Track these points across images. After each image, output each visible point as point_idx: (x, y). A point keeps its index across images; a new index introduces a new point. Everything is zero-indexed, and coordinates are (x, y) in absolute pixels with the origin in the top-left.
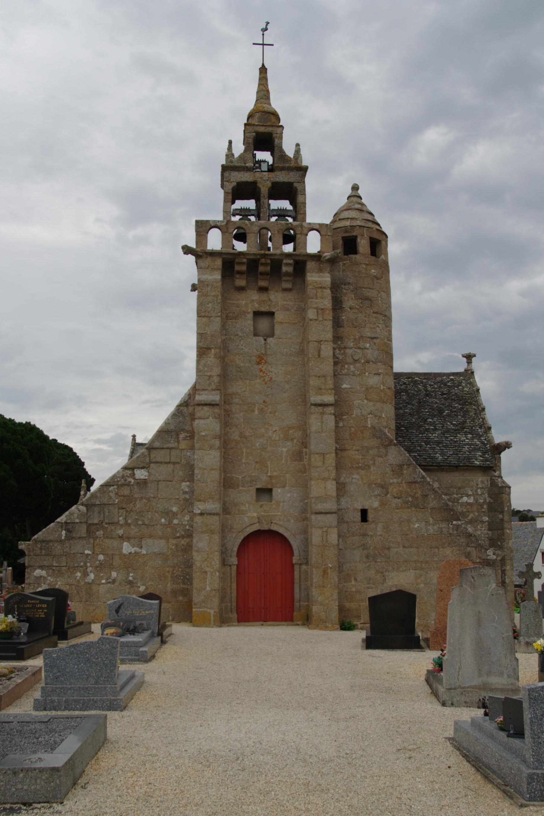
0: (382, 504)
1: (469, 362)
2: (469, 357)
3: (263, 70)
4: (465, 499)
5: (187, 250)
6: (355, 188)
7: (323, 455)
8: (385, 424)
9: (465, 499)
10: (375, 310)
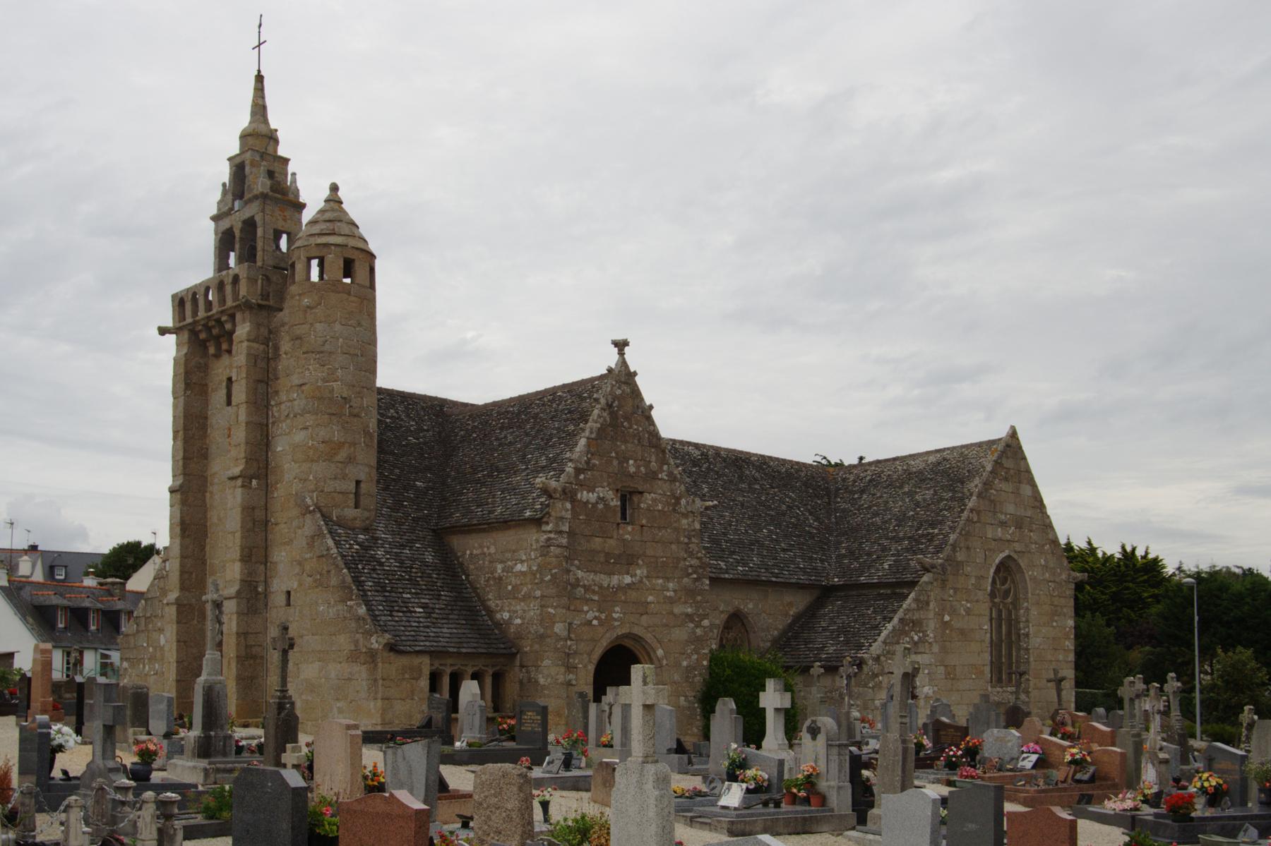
0: (300, 585)
1: (621, 353)
2: (621, 345)
3: (260, 78)
4: (519, 567)
6: (334, 188)
7: (233, 533)
8: (312, 487)
9: (519, 567)
10: (304, 349)
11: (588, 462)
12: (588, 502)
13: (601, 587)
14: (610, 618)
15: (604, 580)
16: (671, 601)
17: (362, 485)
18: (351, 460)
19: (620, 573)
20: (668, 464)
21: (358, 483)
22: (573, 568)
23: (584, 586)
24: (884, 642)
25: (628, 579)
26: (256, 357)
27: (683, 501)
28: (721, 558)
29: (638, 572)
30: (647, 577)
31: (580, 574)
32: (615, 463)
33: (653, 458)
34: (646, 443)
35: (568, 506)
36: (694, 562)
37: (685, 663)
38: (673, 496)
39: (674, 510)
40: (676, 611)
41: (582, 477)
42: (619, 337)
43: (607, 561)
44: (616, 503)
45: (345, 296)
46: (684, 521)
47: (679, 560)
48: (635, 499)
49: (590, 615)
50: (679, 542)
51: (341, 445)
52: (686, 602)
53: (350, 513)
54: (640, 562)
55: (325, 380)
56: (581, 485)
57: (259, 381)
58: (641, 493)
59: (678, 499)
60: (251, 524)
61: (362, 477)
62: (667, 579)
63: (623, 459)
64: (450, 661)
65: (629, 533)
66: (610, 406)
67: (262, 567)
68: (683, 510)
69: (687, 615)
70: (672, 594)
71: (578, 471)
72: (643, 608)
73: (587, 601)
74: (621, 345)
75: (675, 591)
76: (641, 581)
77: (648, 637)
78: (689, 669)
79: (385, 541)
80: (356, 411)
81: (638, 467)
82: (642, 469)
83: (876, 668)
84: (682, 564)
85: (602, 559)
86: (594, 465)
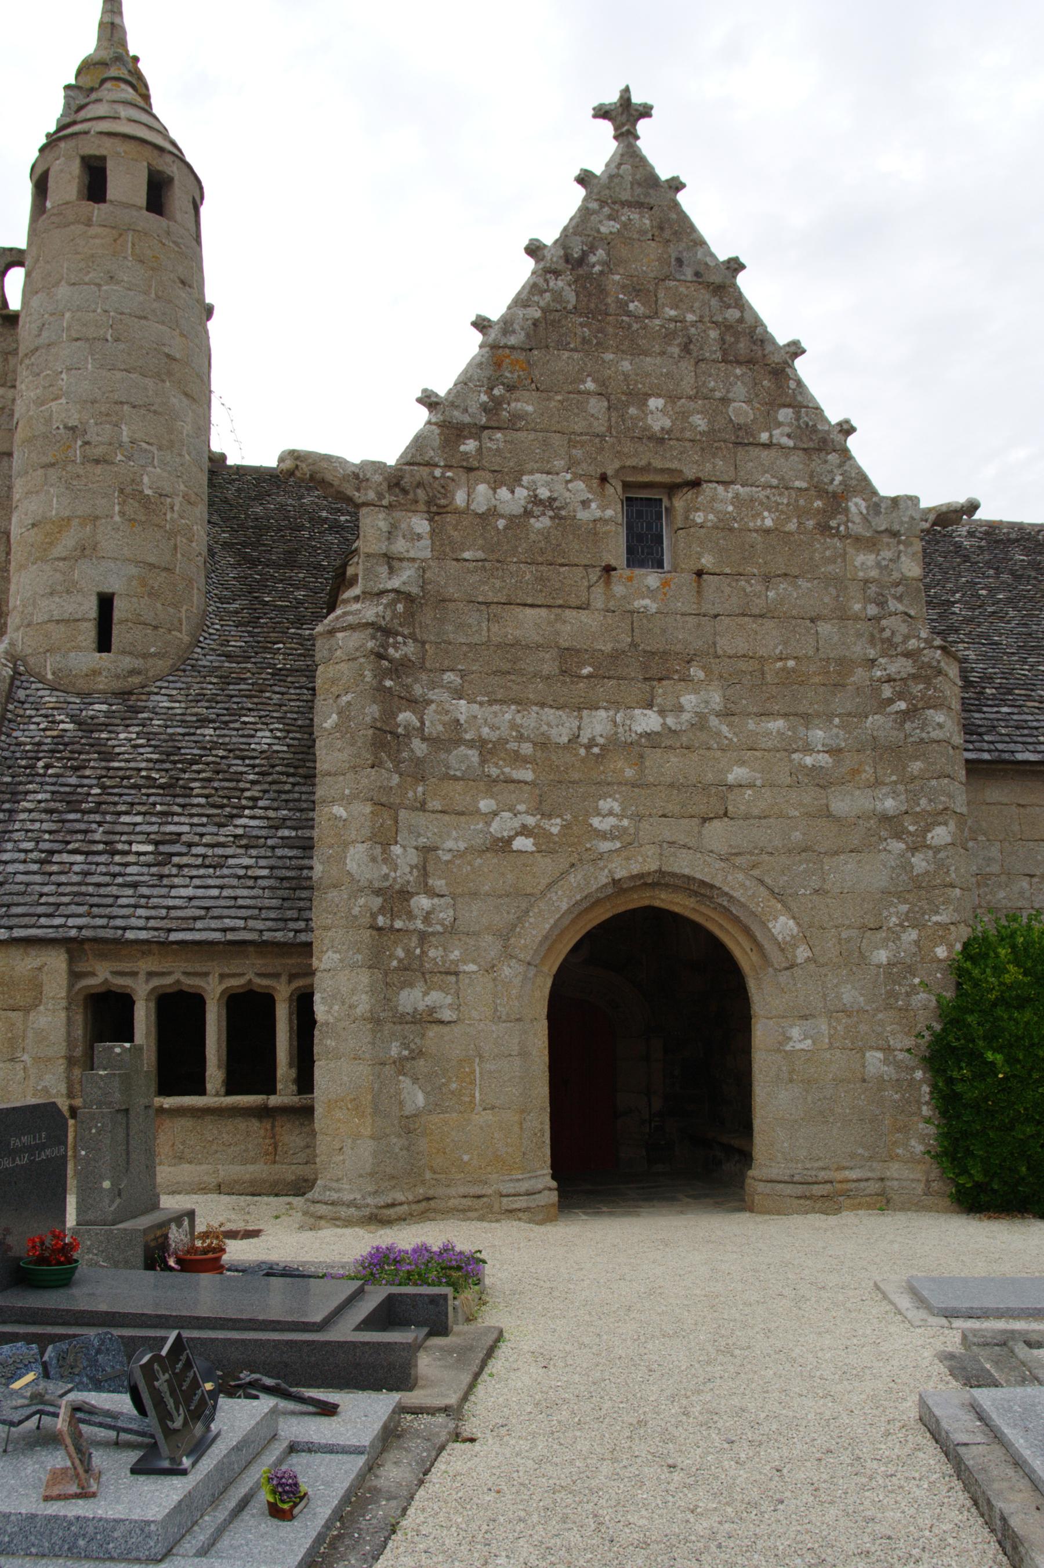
1: (626, 135)
2: (625, 115)
11: (493, 408)
12: (493, 513)
13: (543, 744)
15: (559, 726)
16: (821, 780)
17: (117, 602)
18: (85, 551)
19: (615, 704)
21: (106, 603)
23: (480, 744)
25: (648, 721)
30: (726, 714)
31: (463, 709)
32: (596, 406)
33: (740, 390)
34: (712, 350)
35: (421, 525)
36: (900, 667)
37: (882, 956)
38: (821, 492)
40: (840, 805)
41: (470, 446)
44: (606, 512)
46: (864, 561)
47: (845, 665)
48: (679, 503)
49: (502, 825)
50: (843, 616)
52: (877, 783)
54: (696, 672)
61: (113, 585)
62: (807, 718)
64: (145, 965)
65: (651, 593)
68: (857, 528)
69: (885, 818)
70: (825, 760)
72: (716, 804)
74: (625, 115)
75: (834, 751)
76: (700, 723)
77: (735, 883)
78: (897, 971)
80: (98, 452)
82: (700, 422)
84: (860, 675)
85: (549, 667)
86: (516, 417)
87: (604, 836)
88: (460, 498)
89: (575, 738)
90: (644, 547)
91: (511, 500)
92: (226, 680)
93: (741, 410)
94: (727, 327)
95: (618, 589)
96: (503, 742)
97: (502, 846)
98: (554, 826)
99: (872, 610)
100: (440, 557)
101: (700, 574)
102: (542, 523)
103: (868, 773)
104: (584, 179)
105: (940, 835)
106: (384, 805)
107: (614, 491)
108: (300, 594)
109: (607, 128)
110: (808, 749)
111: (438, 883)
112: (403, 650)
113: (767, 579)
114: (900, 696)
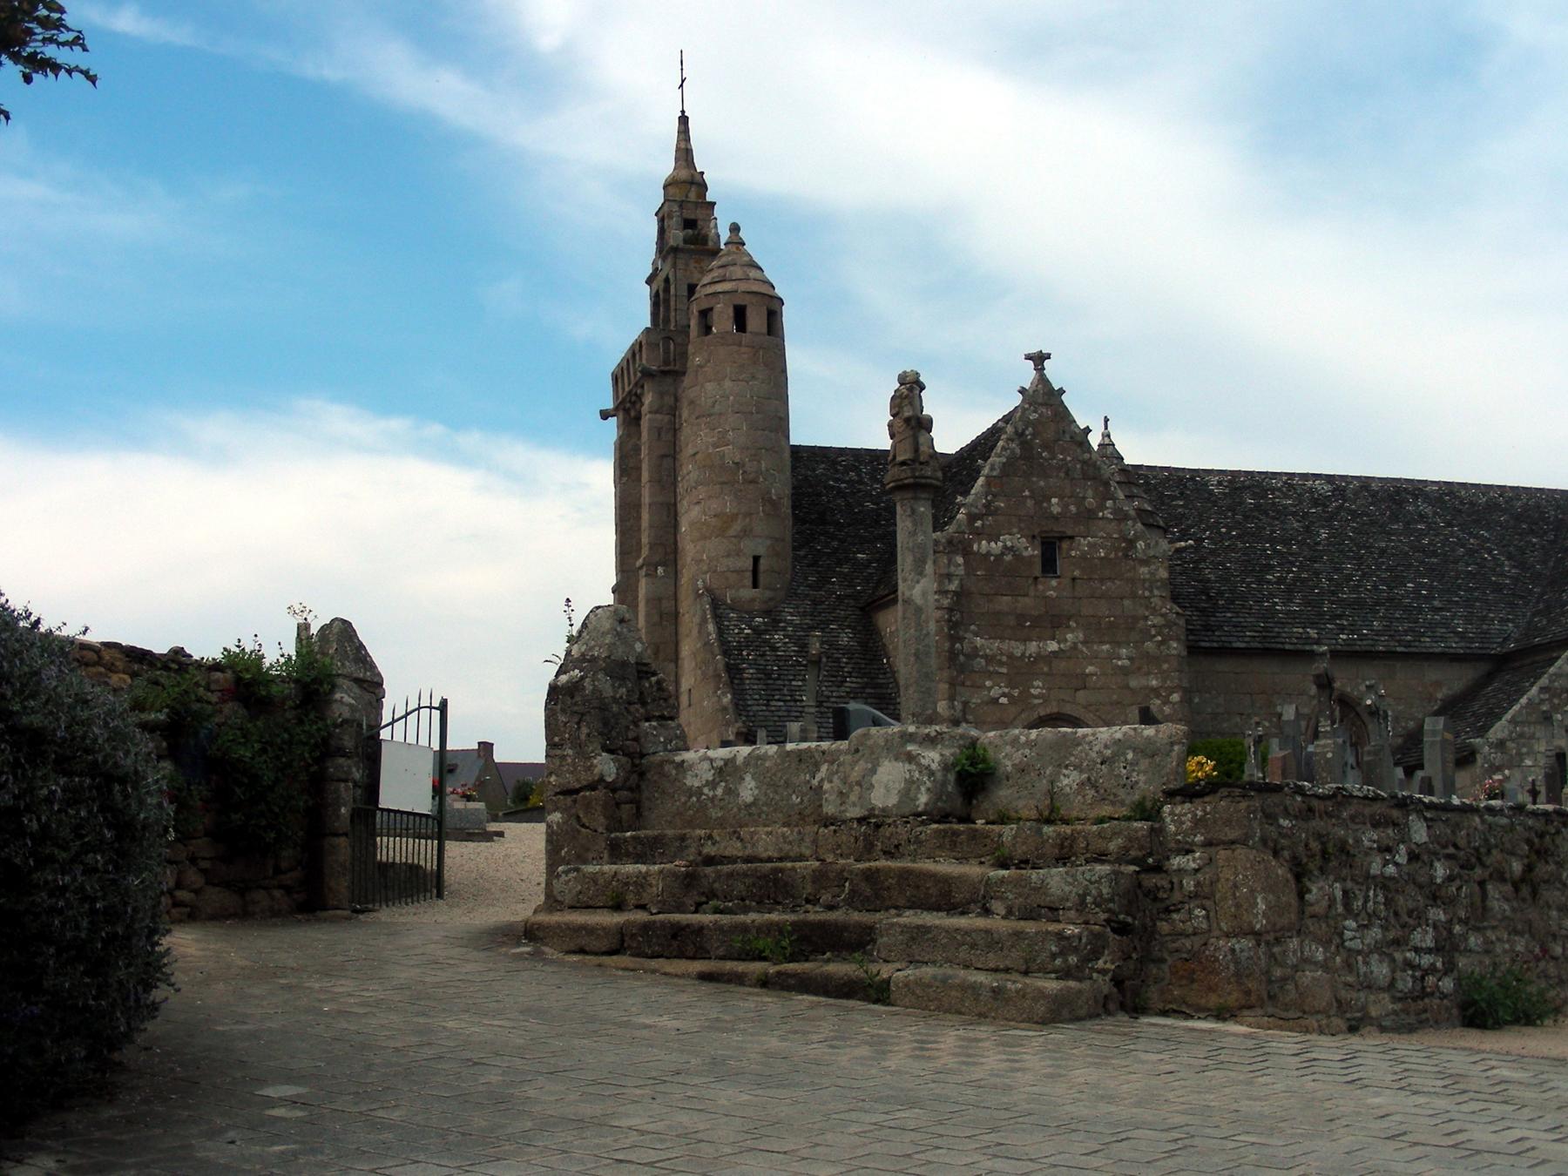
1: (1040, 368)
3: (684, 120)
5: (605, 415)
11: (987, 506)
12: (989, 554)
13: (1011, 656)
14: (1026, 696)
15: (1017, 649)
16: (1125, 671)
17: (762, 561)
18: (745, 533)
19: (1040, 639)
20: (1114, 499)
21: (756, 559)
22: (968, 635)
23: (985, 657)
24: (1513, 721)
25: (1053, 646)
26: (659, 430)
27: (1140, 545)
28: (1313, 625)
29: (1069, 636)
30: (1085, 643)
32: (1030, 503)
33: (1090, 493)
35: (960, 560)
36: (1158, 620)
38: (1125, 539)
39: (1126, 556)
40: (1133, 683)
41: (978, 524)
42: (1034, 350)
43: (1021, 625)
44: (1032, 551)
45: (735, 348)
46: (1144, 570)
47: (1136, 619)
48: (1065, 545)
49: (995, 692)
51: (734, 517)
52: (1148, 674)
53: (747, 593)
54: (1073, 624)
55: (715, 446)
56: (979, 534)
57: (664, 456)
58: (1072, 538)
59: (1131, 543)
60: (656, 618)
61: (761, 551)
62: (1119, 644)
63: (1042, 498)
65: (1054, 589)
66: (1020, 435)
67: (672, 666)
68: (1140, 556)
70: (1126, 662)
71: (972, 518)
73: (990, 675)
74: (1039, 359)
75: (1129, 658)
76: (1074, 647)
79: (790, 623)
81: (1066, 506)
82: (1073, 508)
83: (1497, 758)
84: (1141, 624)
85: (1013, 623)
86: (997, 508)
87: (1036, 697)
88: (975, 547)
89: (1023, 654)
90: (1049, 564)
91: (996, 547)
92: (815, 603)
93: (1090, 501)
94: (1084, 462)
95: (1040, 587)
96: (993, 657)
97: (995, 701)
98: (1016, 693)
99: (1147, 594)
100: (968, 574)
101: (1074, 579)
102: (1008, 558)
103: (1145, 668)
104: (1022, 391)
105: (1175, 697)
106: (952, 684)
107: (1037, 542)
108: (835, 544)
109: (1031, 363)
110: (1119, 658)
111: (970, 717)
112: (957, 617)
113: (1102, 581)
114: (1159, 634)
